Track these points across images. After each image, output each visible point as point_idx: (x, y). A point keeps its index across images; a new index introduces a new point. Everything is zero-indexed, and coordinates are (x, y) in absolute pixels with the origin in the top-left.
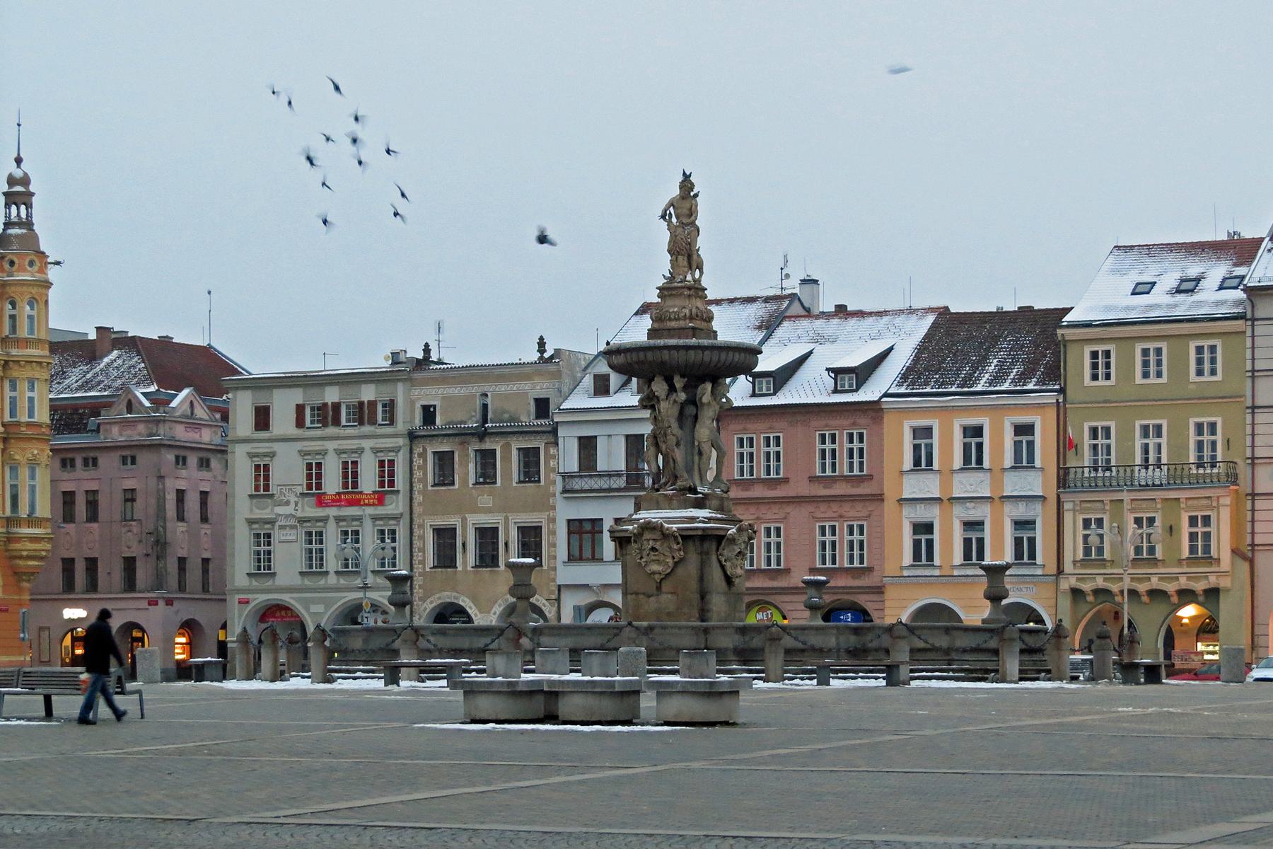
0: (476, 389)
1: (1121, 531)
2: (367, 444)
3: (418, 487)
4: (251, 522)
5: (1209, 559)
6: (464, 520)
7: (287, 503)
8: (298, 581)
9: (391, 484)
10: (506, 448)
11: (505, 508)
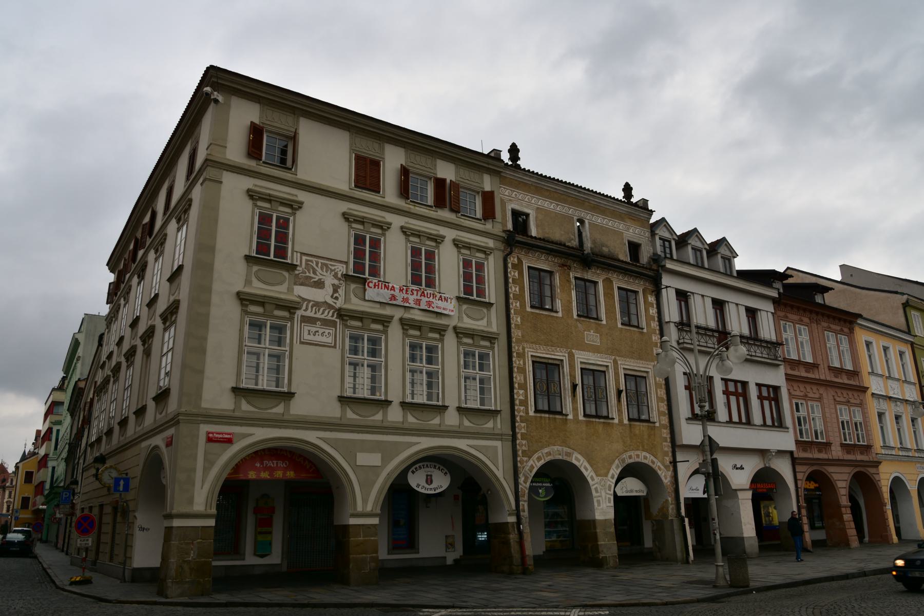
2: (450, 234)
3: (515, 305)
4: (244, 299)
6: (571, 356)
7: (320, 284)
9: (481, 293)
10: (608, 282)
11: (613, 351)
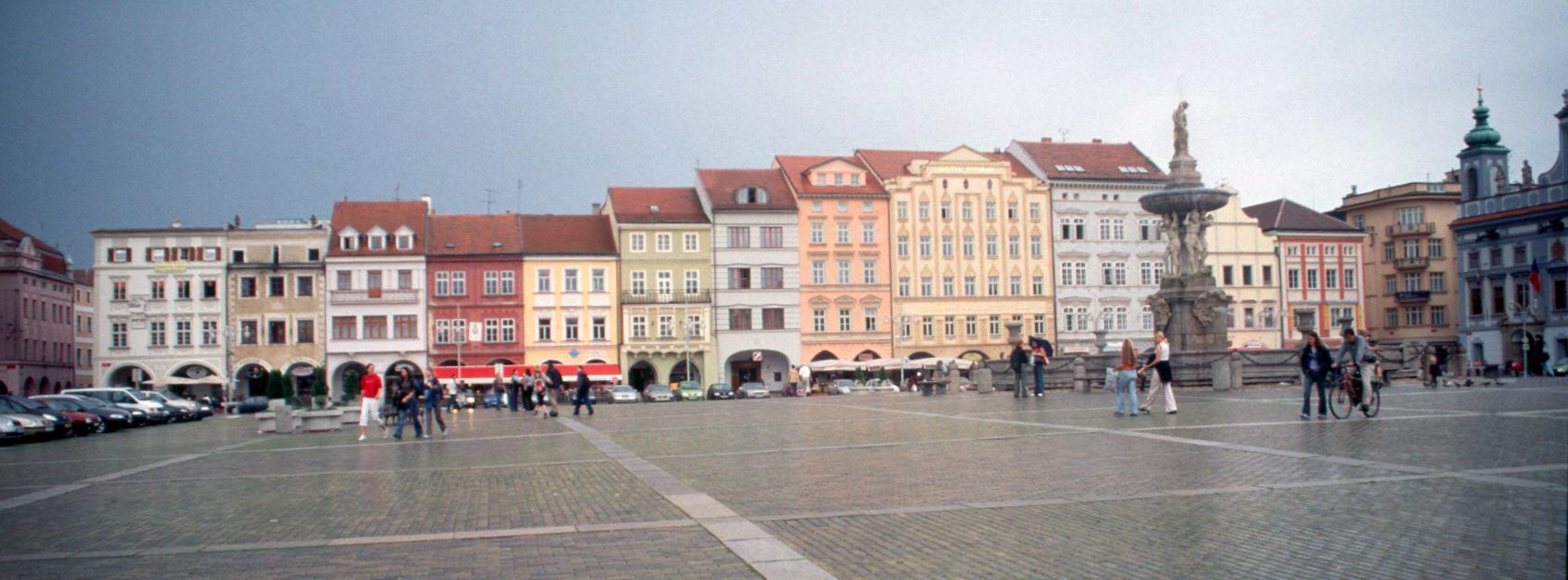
0: (271, 243)
1: (653, 324)
2: (196, 272)
4: (111, 317)
5: (698, 338)
8: (146, 353)
10: (291, 277)
11: (291, 310)
